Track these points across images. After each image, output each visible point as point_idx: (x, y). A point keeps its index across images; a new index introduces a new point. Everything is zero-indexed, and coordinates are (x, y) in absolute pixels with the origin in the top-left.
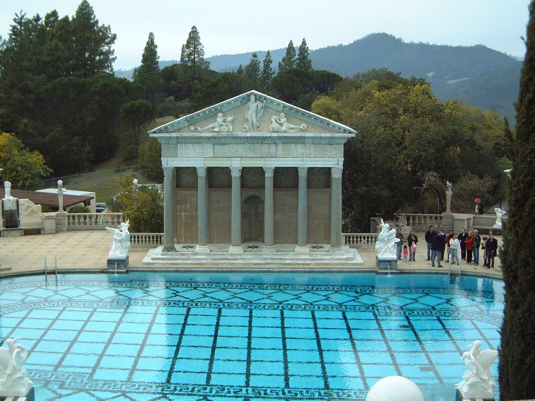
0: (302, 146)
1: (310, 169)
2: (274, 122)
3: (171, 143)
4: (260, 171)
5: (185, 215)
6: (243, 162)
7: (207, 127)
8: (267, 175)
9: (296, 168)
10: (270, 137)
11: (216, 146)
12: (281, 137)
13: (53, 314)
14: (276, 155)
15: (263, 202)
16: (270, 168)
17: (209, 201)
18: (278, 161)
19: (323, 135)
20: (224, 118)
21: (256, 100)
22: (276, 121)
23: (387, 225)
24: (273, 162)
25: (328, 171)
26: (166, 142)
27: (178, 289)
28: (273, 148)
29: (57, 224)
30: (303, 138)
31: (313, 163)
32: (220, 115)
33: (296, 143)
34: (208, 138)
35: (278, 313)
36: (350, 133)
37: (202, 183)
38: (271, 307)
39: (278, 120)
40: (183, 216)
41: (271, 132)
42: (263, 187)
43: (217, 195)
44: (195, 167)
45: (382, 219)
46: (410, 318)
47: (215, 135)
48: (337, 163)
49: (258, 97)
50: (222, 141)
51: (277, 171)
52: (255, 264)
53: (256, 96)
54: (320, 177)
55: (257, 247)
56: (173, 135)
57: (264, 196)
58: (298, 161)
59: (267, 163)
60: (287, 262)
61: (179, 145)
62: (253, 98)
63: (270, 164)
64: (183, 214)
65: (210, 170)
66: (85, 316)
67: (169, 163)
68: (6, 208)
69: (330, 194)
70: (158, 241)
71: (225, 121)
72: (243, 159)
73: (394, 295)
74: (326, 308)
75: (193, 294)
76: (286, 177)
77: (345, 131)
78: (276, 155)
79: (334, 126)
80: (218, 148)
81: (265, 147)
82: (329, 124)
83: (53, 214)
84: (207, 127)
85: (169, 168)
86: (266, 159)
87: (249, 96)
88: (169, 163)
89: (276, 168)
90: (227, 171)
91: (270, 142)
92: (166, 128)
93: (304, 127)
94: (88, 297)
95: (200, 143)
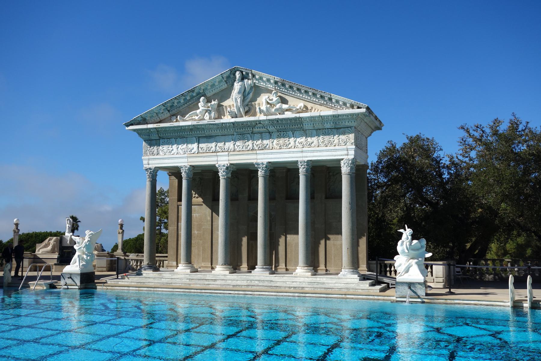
3: (153, 138)
6: (231, 158)
16: (263, 164)
18: (272, 153)
19: (323, 114)
24: (266, 156)
31: (315, 154)
32: (202, 98)
36: (358, 108)
47: (195, 123)
48: (346, 152)
49: (244, 73)
50: (207, 133)
52: (234, 286)
53: (242, 72)
54: (324, 175)
56: (150, 126)
58: (297, 152)
59: (259, 157)
60: (278, 284)
61: (161, 141)
62: (238, 75)
68: (64, 245)
72: (231, 153)
76: (283, 176)
79: (337, 102)
85: (150, 169)
86: (258, 152)
88: (150, 162)
91: (261, 130)
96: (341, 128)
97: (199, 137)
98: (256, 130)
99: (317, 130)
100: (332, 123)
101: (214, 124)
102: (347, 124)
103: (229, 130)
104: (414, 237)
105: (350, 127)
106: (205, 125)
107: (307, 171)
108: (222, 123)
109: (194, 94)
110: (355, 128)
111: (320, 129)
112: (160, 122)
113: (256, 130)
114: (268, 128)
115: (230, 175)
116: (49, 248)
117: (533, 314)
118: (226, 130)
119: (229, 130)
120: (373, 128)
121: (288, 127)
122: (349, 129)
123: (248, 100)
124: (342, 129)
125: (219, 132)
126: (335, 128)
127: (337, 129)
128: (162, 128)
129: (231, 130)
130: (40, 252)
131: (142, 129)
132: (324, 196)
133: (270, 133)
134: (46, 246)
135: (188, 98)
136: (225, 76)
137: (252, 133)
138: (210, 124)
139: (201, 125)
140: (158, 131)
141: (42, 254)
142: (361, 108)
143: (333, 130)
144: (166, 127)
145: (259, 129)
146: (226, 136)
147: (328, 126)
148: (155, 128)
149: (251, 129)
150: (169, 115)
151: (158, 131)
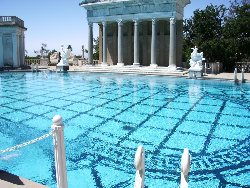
0: (153, 5)
11: (110, 9)
14: (139, 12)
28: (138, 8)
33: (149, 5)
50: (113, 7)
78: (139, 12)
80: (111, 10)
97: (109, 8)
98: (133, 5)
99: (160, 4)
101: (115, 3)
104: (199, 51)
105: (174, 3)
106: (112, 3)
107: (155, 23)
108: (119, 2)
110: (176, 3)
111: (161, 4)
112: (93, 2)
113: (133, 5)
114: (138, 4)
115: (122, 25)
116: (55, 57)
117: (242, 84)
120: (186, 3)
122: (173, 4)
124: (170, 4)
125: (118, 6)
126: (167, 3)
127: (168, 4)
128: (94, 5)
130: (51, 59)
131: (86, 6)
132: (164, 34)
134: (55, 55)
137: (132, 6)
138: (114, 3)
139: (110, 3)
140: (92, 6)
141: (52, 59)
143: (167, 4)
144: (95, 5)
145: (134, 4)
146: (121, 8)
148: (91, 5)
151: (92, 6)
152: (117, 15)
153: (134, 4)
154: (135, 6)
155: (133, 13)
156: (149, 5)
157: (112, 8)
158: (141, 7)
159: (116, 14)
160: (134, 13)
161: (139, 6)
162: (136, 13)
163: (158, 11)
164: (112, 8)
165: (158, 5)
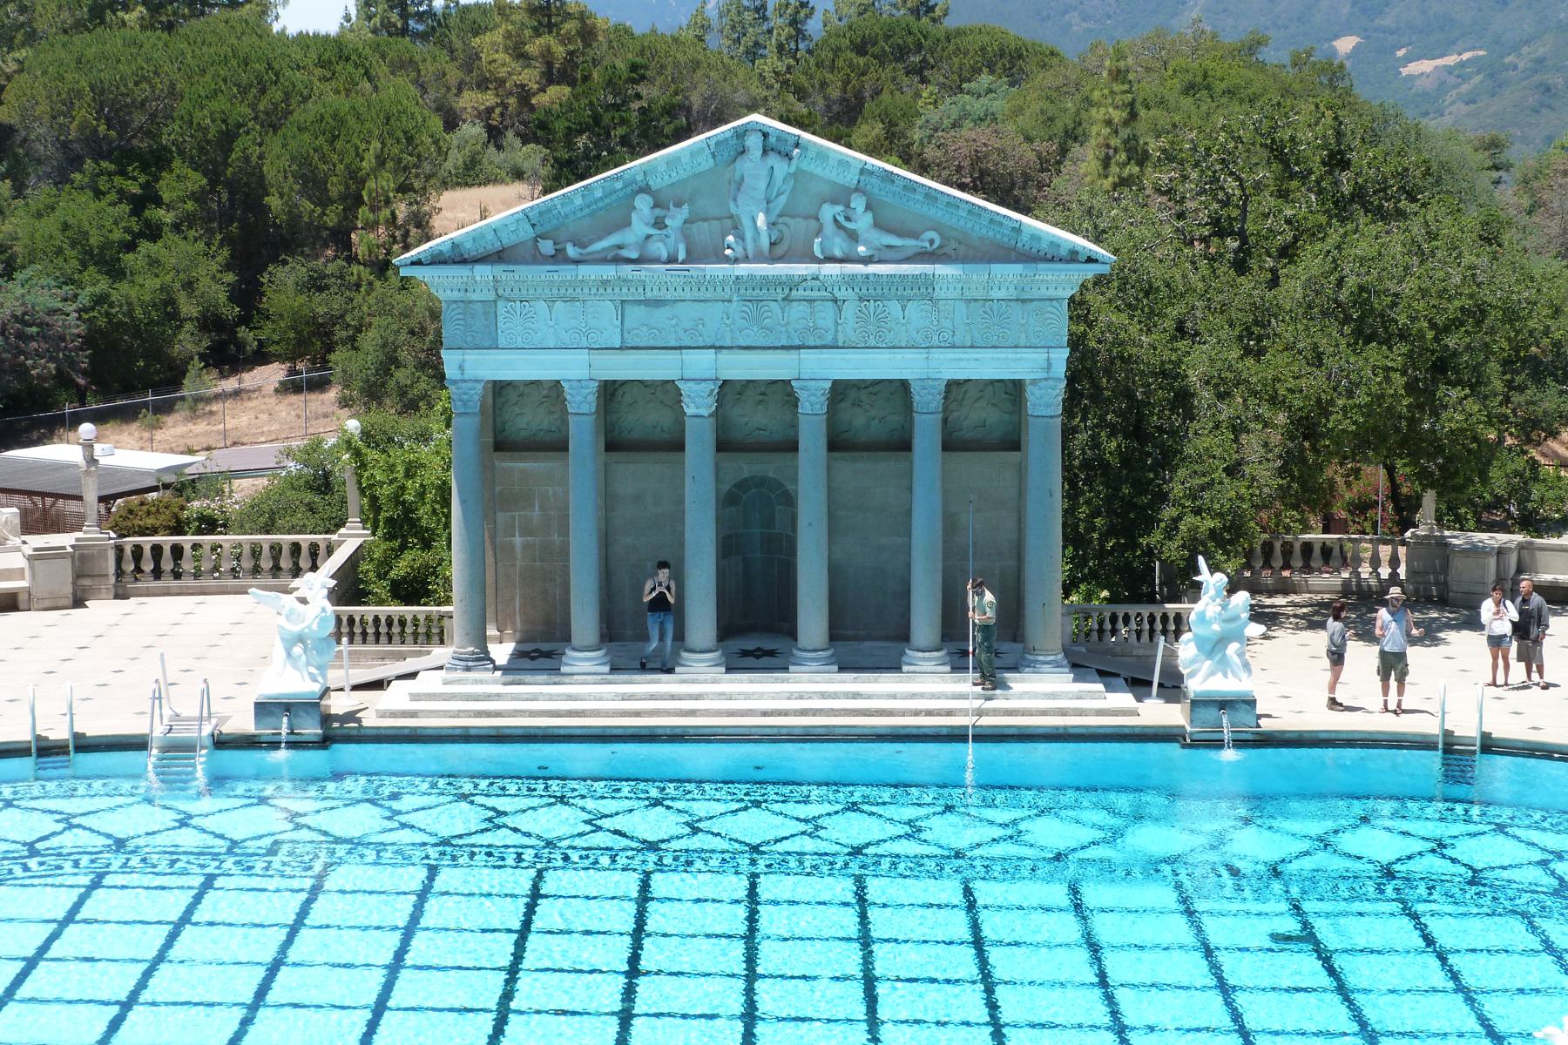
0: (927, 305)
1: (953, 386)
2: (829, 228)
3: (474, 297)
4: (783, 392)
5: (526, 547)
7: (598, 246)
8: (805, 407)
9: (904, 385)
10: (816, 278)
11: (628, 308)
12: (853, 277)
13: (58, 902)
14: (835, 339)
15: (789, 500)
17: (608, 502)
20: (658, 212)
21: (765, 152)
22: (836, 221)
23: (1220, 579)
25: (1014, 391)
26: (456, 295)
27: (501, 803)
28: (826, 313)
29: (78, 575)
30: (928, 282)
32: (643, 203)
33: (904, 301)
34: (605, 283)
35: (843, 888)
36: (1090, 260)
37: (583, 433)
38: (824, 864)
39: (841, 219)
40: (518, 549)
41: (820, 261)
42: (792, 446)
43: (637, 474)
44: (557, 384)
45: (1201, 559)
46: (1307, 906)
49: (772, 140)
51: (841, 391)
53: (765, 135)
55: (771, 653)
57: (795, 480)
62: (754, 142)
63: (817, 370)
64: (518, 540)
65: (610, 391)
66: (174, 905)
67: (470, 366)
69: (1021, 471)
70: (433, 633)
71: (659, 224)
73: (1247, 821)
74: (1010, 869)
75: (557, 822)
77: (1073, 257)
78: (835, 339)
80: (635, 314)
81: (798, 310)
82: (1018, 229)
83: (65, 540)
84: (598, 246)
87: (741, 134)
89: (836, 384)
90: (668, 392)
91: (815, 294)
92: (455, 245)
93: (932, 242)
94: (188, 839)
95: (573, 300)
96: (1032, 300)
99: (969, 301)
100: (1012, 289)
102: (1051, 293)
103: (719, 289)
109: (619, 185)
118: (711, 289)
119: (719, 289)
121: (893, 289)
123: (777, 212)
127: (1024, 301)
129: (727, 289)
133: (835, 301)
135: (598, 194)
136: (712, 143)
142: (1096, 261)
145: (808, 293)
147: (1002, 294)
149: (787, 291)
150: (531, 233)
152: (681, 348)
153: (808, 293)
154: (811, 301)
155: (799, 347)
156: (904, 301)
157: (647, 302)
158: (850, 310)
159: (673, 343)
160: (797, 342)
161: (835, 301)
162: (812, 343)
163: (958, 342)
164: (647, 302)
165: (962, 306)
